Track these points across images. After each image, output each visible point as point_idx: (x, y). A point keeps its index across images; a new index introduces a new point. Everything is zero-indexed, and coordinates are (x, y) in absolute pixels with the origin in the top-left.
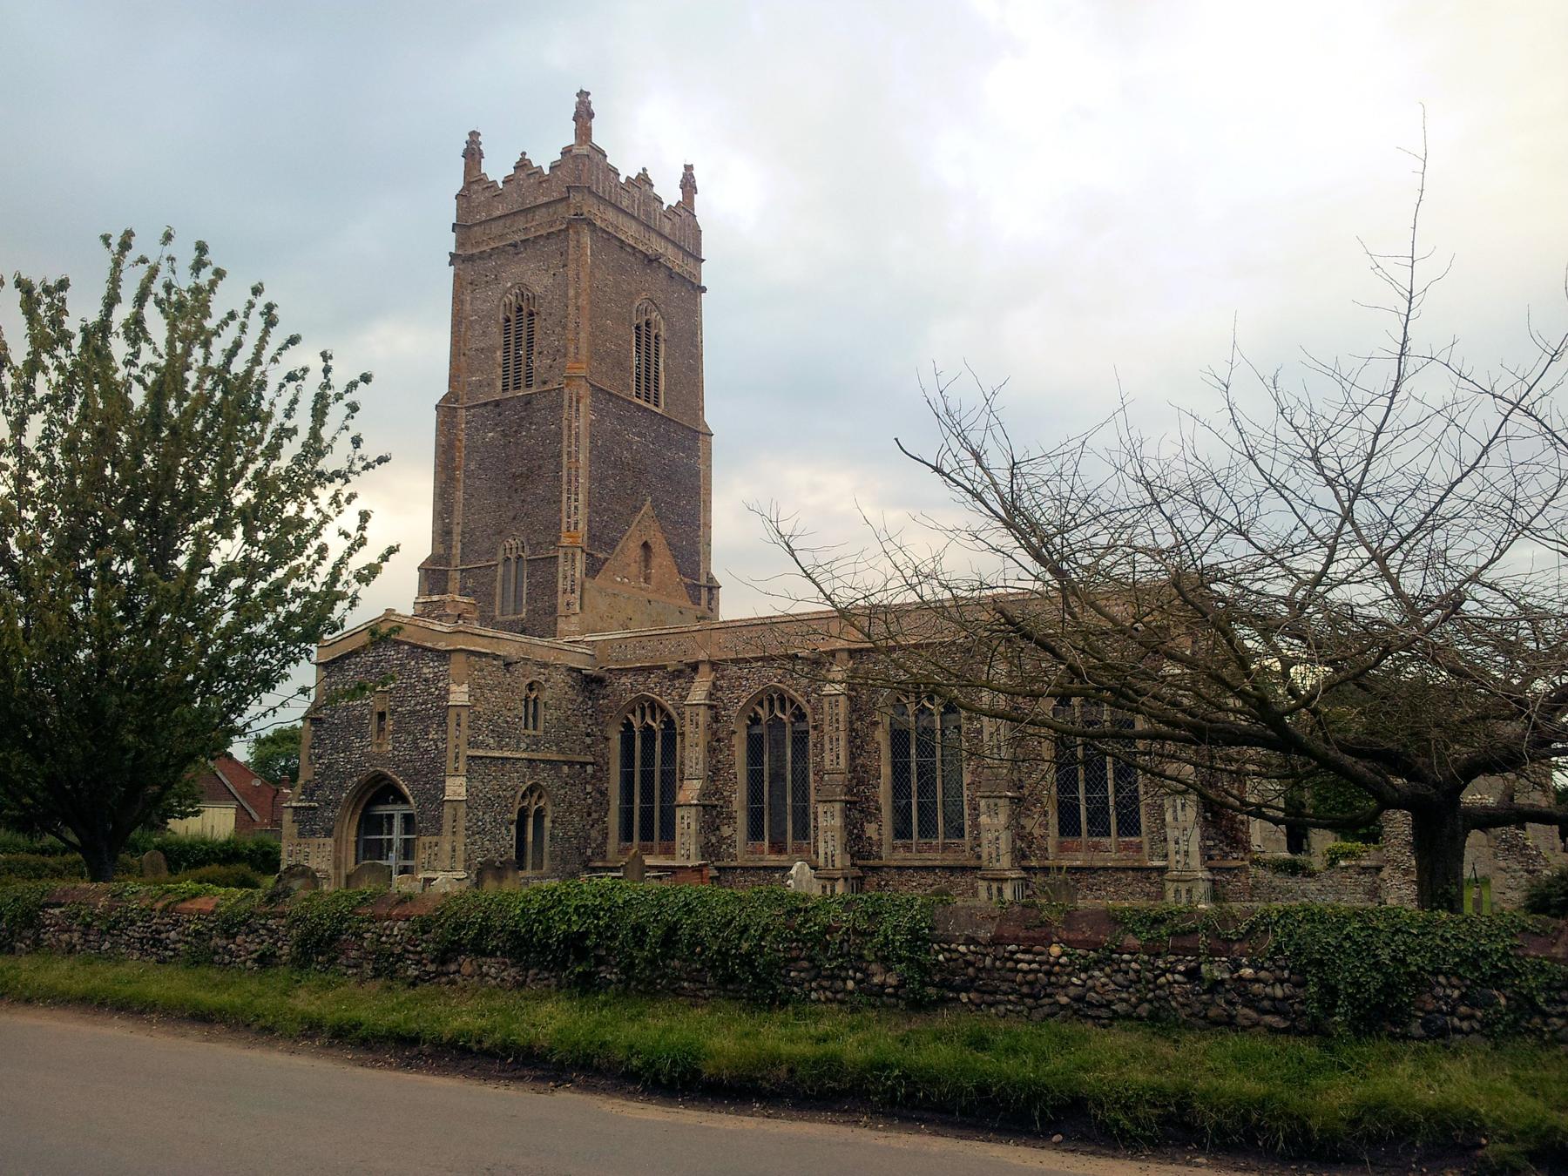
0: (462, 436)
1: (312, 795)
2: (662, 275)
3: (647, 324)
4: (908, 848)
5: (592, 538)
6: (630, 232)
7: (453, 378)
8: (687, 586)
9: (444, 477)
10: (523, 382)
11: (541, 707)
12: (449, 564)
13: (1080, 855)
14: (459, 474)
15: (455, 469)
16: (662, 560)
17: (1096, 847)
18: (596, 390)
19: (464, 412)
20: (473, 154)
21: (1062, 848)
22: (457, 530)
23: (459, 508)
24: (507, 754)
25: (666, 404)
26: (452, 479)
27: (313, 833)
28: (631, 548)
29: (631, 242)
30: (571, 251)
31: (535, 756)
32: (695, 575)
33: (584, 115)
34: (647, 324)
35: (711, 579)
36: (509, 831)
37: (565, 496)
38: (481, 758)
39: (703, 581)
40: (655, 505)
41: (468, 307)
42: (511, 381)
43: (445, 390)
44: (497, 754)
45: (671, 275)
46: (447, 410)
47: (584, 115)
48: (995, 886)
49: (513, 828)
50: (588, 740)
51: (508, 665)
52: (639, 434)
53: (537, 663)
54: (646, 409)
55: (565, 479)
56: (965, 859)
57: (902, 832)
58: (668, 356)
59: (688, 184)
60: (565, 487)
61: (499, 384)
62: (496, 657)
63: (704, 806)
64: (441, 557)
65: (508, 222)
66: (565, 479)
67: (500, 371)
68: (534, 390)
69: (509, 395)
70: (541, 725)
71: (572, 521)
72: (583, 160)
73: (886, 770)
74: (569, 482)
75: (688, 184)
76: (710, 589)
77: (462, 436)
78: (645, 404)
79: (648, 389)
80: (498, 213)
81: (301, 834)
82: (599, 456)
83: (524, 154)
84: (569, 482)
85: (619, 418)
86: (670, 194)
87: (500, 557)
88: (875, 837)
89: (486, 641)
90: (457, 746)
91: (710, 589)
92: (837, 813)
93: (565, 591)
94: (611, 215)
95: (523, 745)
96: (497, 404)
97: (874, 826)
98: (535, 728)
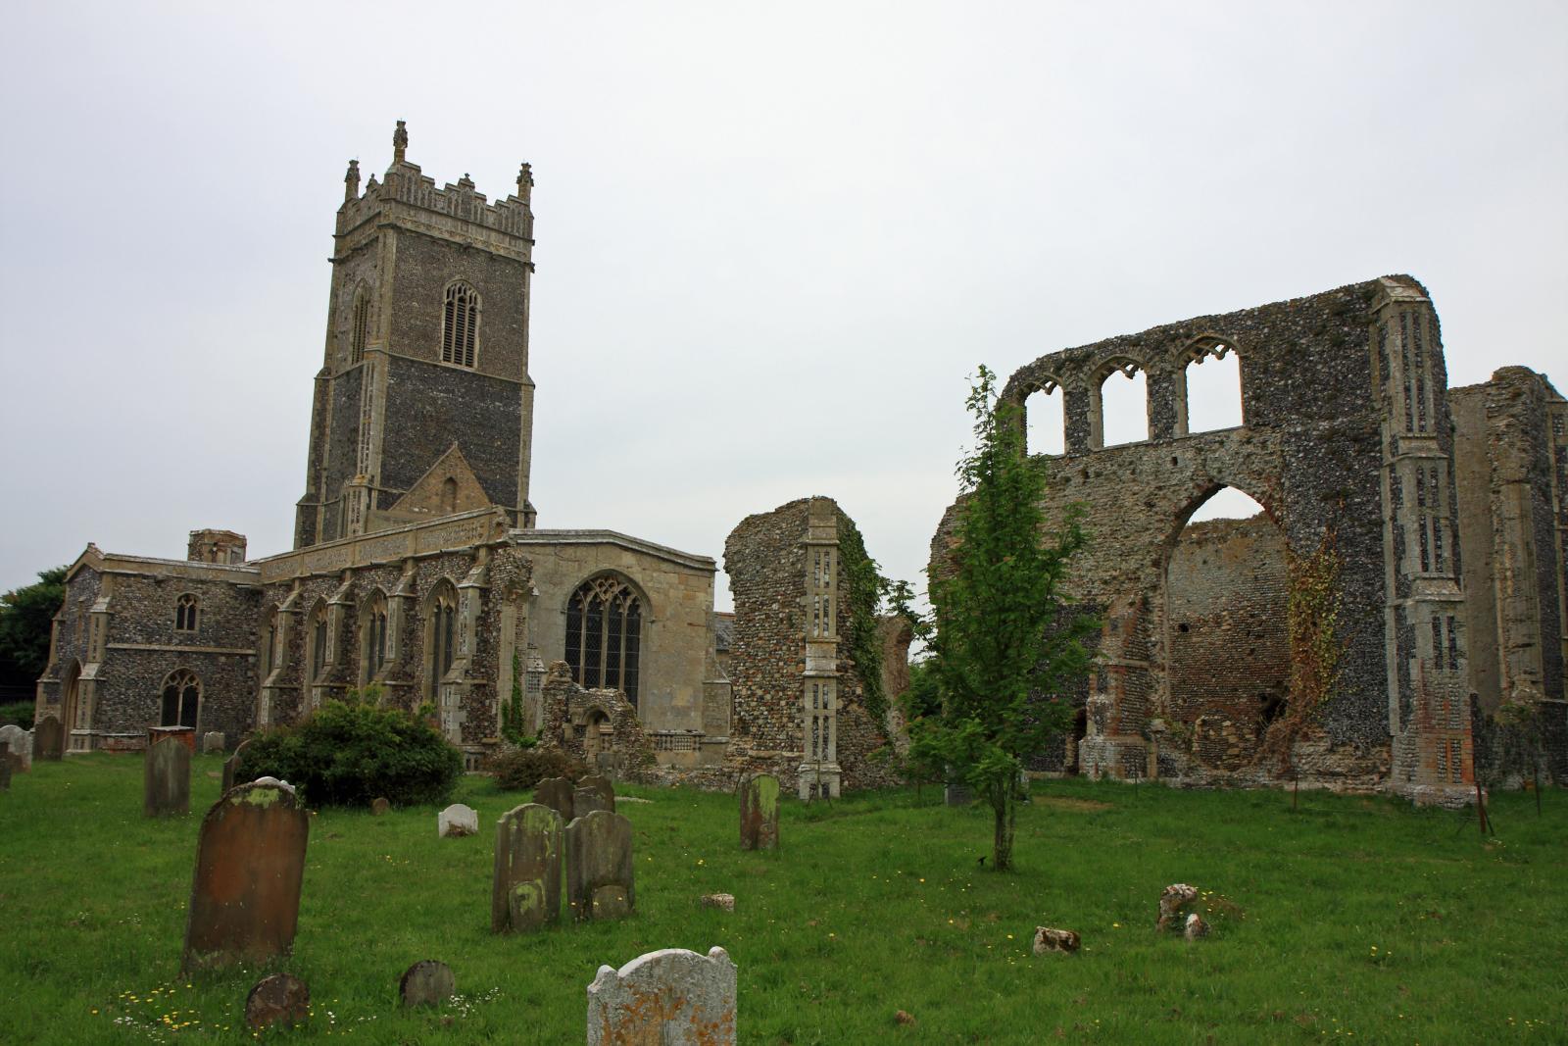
1: (57, 674)
2: (481, 259)
3: (462, 300)
5: (386, 478)
6: (443, 229)
7: (329, 356)
9: (317, 433)
11: (198, 613)
12: (318, 501)
14: (328, 431)
18: (394, 360)
20: (352, 177)
23: (326, 456)
24: (157, 647)
25: (480, 364)
28: (434, 482)
29: (446, 236)
31: (187, 649)
33: (401, 138)
35: (527, 505)
36: (155, 703)
38: (125, 650)
39: (520, 506)
40: (463, 447)
41: (340, 300)
43: (320, 365)
44: (142, 647)
45: (492, 258)
46: (322, 381)
47: (401, 138)
49: (160, 702)
50: (252, 638)
51: (159, 583)
52: (447, 391)
53: (192, 581)
54: (454, 370)
58: (485, 324)
59: (525, 179)
60: (360, 438)
61: (350, 359)
62: (145, 577)
63: (281, 689)
64: (312, 495)
67: (351, 348)
70: (197, 626)
71: (364, 465)
72: (405, 177)
74: (364, 435)
75: (525, 179)
76: (527, 514)
78: (459, 367)
79: (459, 353)
80: (358, 223)
81: (48, 702)
82: (393, 411)
83: (373, 175)
84: (364, 435)
85: (423, 380)
86: (496, 188)
89: (135, 565)
90: (95, 641)
91: (527, 514)
93: (352, 521)
94: (423, 217)
95: (175, 641)
96: (348, 373)
98: (191, 626)
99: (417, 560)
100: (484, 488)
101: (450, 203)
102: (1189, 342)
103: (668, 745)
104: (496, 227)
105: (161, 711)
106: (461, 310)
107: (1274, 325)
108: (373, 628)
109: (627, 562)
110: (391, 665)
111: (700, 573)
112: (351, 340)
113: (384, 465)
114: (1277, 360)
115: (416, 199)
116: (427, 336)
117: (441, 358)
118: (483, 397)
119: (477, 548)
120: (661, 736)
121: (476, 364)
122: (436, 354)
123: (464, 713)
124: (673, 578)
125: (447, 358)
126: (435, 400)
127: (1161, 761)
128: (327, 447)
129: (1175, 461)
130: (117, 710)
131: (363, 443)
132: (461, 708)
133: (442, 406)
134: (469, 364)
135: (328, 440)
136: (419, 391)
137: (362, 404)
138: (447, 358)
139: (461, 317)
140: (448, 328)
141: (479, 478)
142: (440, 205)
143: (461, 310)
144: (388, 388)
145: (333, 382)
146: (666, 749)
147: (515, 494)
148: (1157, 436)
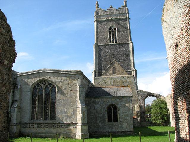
34: (113, 30)
78: (113, 43)
100: (123, 68)
103: (64, 126)
106: (113, 32)
111: (75, 75)
113: (98, 67)
116: (106, 39)
117: (109, 42)
120: (61, 124)
122: (108, 42)
124: (64, 78)
125: (110, 42)
126: (108, 51)
133: (110, 52)
134: (116, 42)
142: (106, 13)
144: (98, 52)
146: (63, 128)
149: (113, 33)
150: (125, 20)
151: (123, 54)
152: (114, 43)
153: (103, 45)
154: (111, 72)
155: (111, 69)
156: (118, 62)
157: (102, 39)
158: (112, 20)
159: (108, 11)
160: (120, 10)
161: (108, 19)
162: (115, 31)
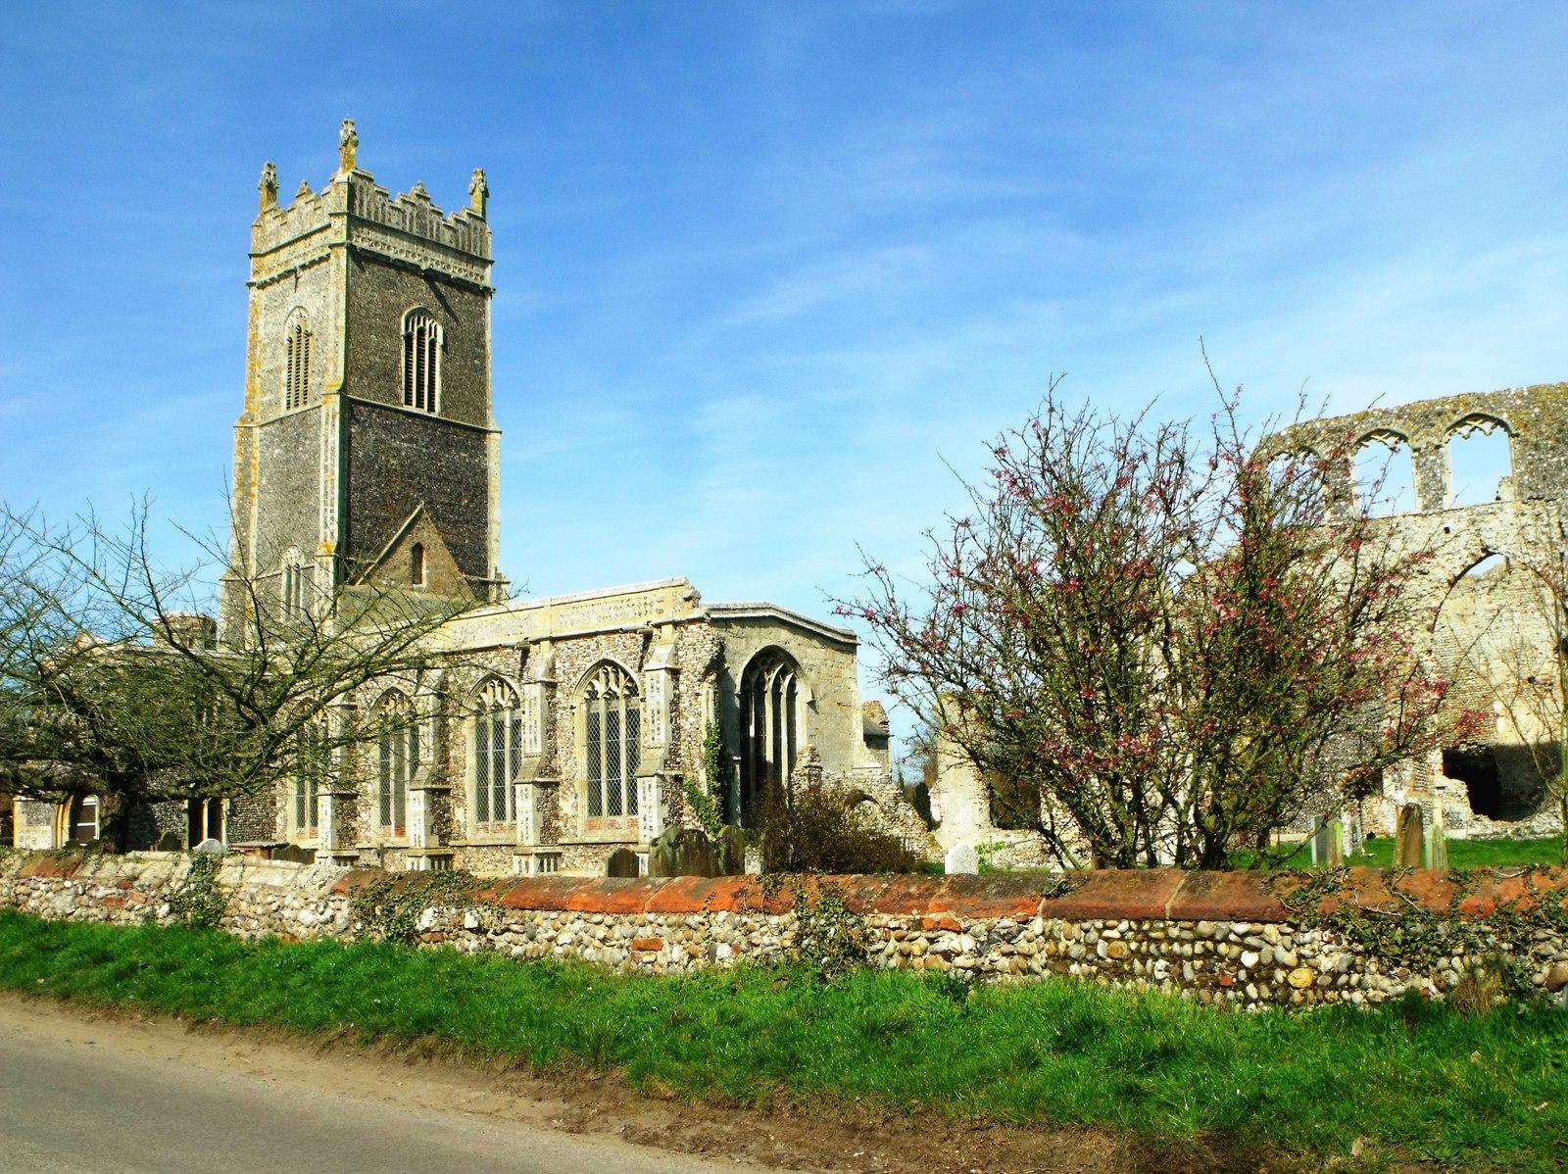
0: (257, 454)
3: (421, 332)
4: (486, 828)
8: (470, 583)
10: (301, 399)
13: (600, 832)
14: (255, 490)
15: (250, 485)
16: (438, 560)
17: (612, 824)
19: (257, 431)
21: (591, 827)
22: (253, 542)
26: (249, 494)
27: (38, 821)
28: (404, 553)
30: (332, 274)
32: (482, 569)
34: (421, 332)
37: (322, 507)
39: (492, 577)
42: (292, 400)
48: (524, 859)
49: (185, 817)
52: (410, 441)
55: (322, 492)
56: (502, 838)
57: (482, 815)
60: (322, 499)
61: (284, 403)
65: (292, 248)
66: (322, 492)
67: (284, 390)
68: (308, 406)
69: (290, 412)
73: (471, 761)
77: (257, 454)
81: (29, 823)
85: (385, 428)
87: (283, 566)
88: (462, 821)
92: (422, 800)
96: (281, 420)
97: (461, 810)
99: (553, 640)
100: (454, 556)
101: (404, 218)
102: (1456, 418)
104: (453, 245)
105: (187, 828)
106: (421, 343)
107: (1544, 407)
108: (592, 720)
109: (780, 637)
110: (538, 759)
112: (285, 380)
114: (1548, 438)
115: (369, 213)
116: (388, 374)
117: (403, 401)
118: (448, 446)
119: (658, 626)
121: (437, 408)
122: (397, 397)
123: (666, 808)
126: (398, 450)
127: (1446, 815)
128: (255, 510)
129: (1447, 530)
130: (144, 828)
131: (325, 503)
132: (663, 802)
134: (431, 408)
135: (256, 501)
136: (383, 442)
137: (322, 458)
138: (408, 402)
139: (420, 353)
140: (408, 366)
141: (448, 544)
142: (394, 221)
143: (421, 343)
145: (257, 431)
147: (485, 561)
148: (1426, 507)
149: (420, 353)
150: (485, 292)
151: (460, 482)
152: (424, 411)
153: (374, 406)
154: (405, 570)
155: (404, 553)
156: (436, 517)
157: (370, 367)
158: (431, 276)
159: (409, 209)
160: (461, 228)
161: (402, 257)
162: (433, 343)
